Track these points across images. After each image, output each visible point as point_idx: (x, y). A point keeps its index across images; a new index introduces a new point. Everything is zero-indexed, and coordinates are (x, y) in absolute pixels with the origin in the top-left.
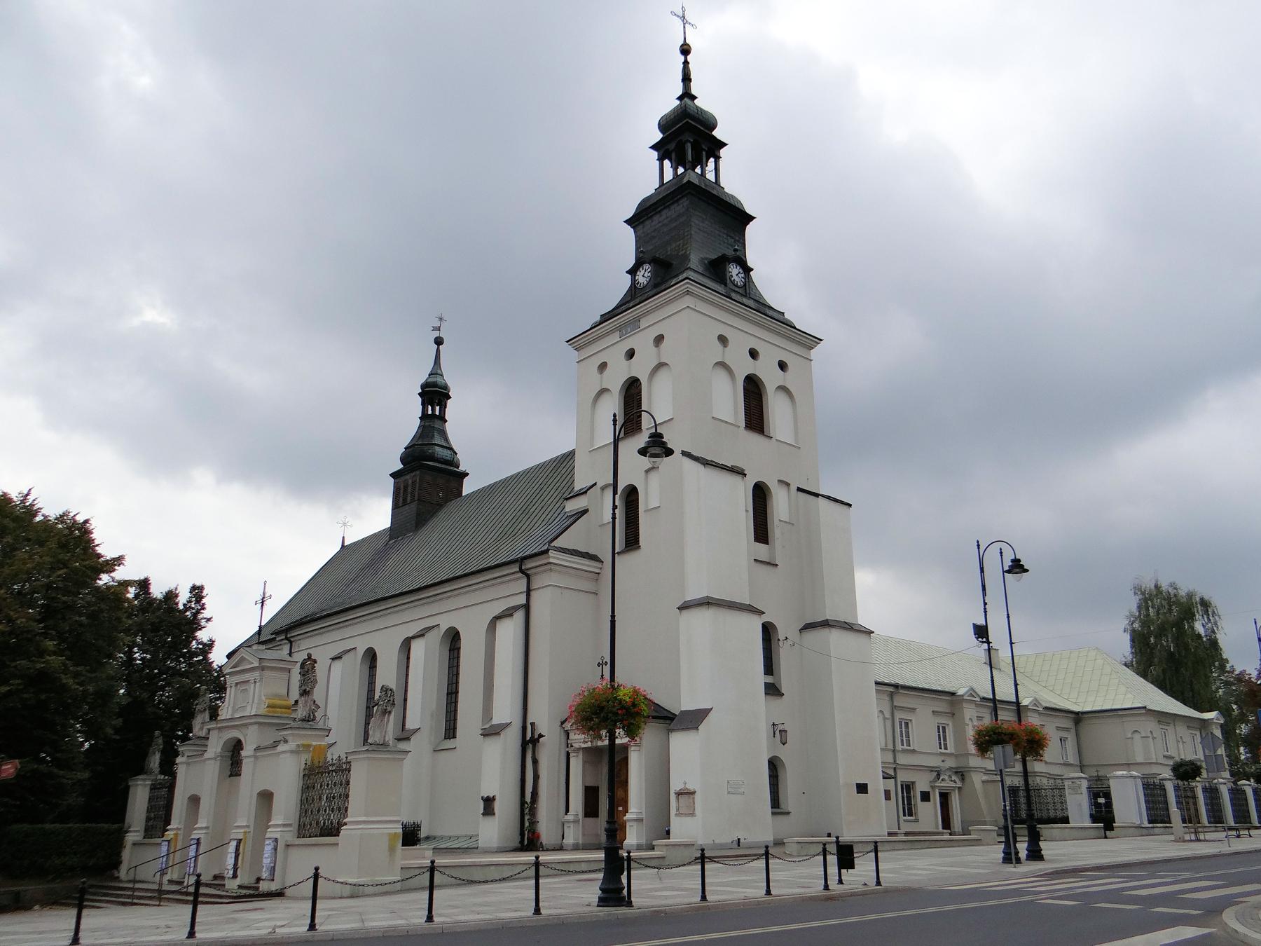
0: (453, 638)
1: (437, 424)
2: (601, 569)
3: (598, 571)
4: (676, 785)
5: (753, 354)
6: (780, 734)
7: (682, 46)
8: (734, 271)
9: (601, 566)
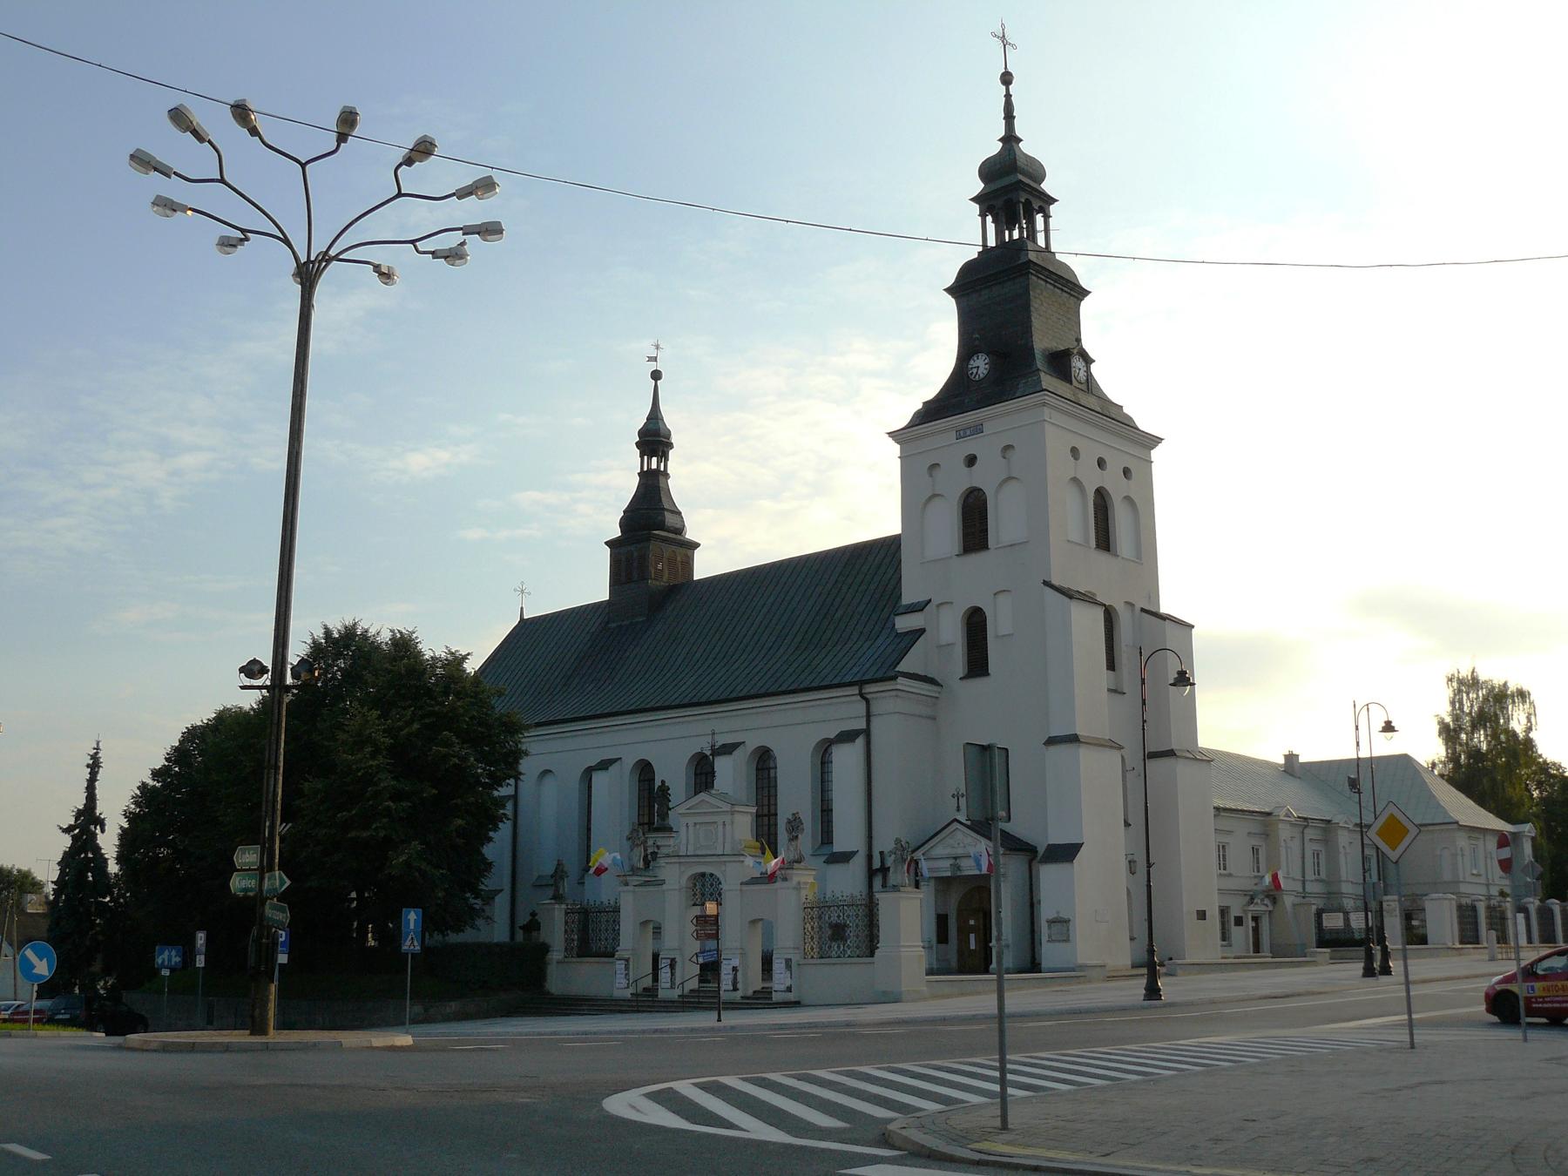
0: (764, 761)
2: (939, 693)
3: (937, 695)
4: (1046, 912)
5: (1101, 463)
7: (1003, 74)
8: (1077, 363)
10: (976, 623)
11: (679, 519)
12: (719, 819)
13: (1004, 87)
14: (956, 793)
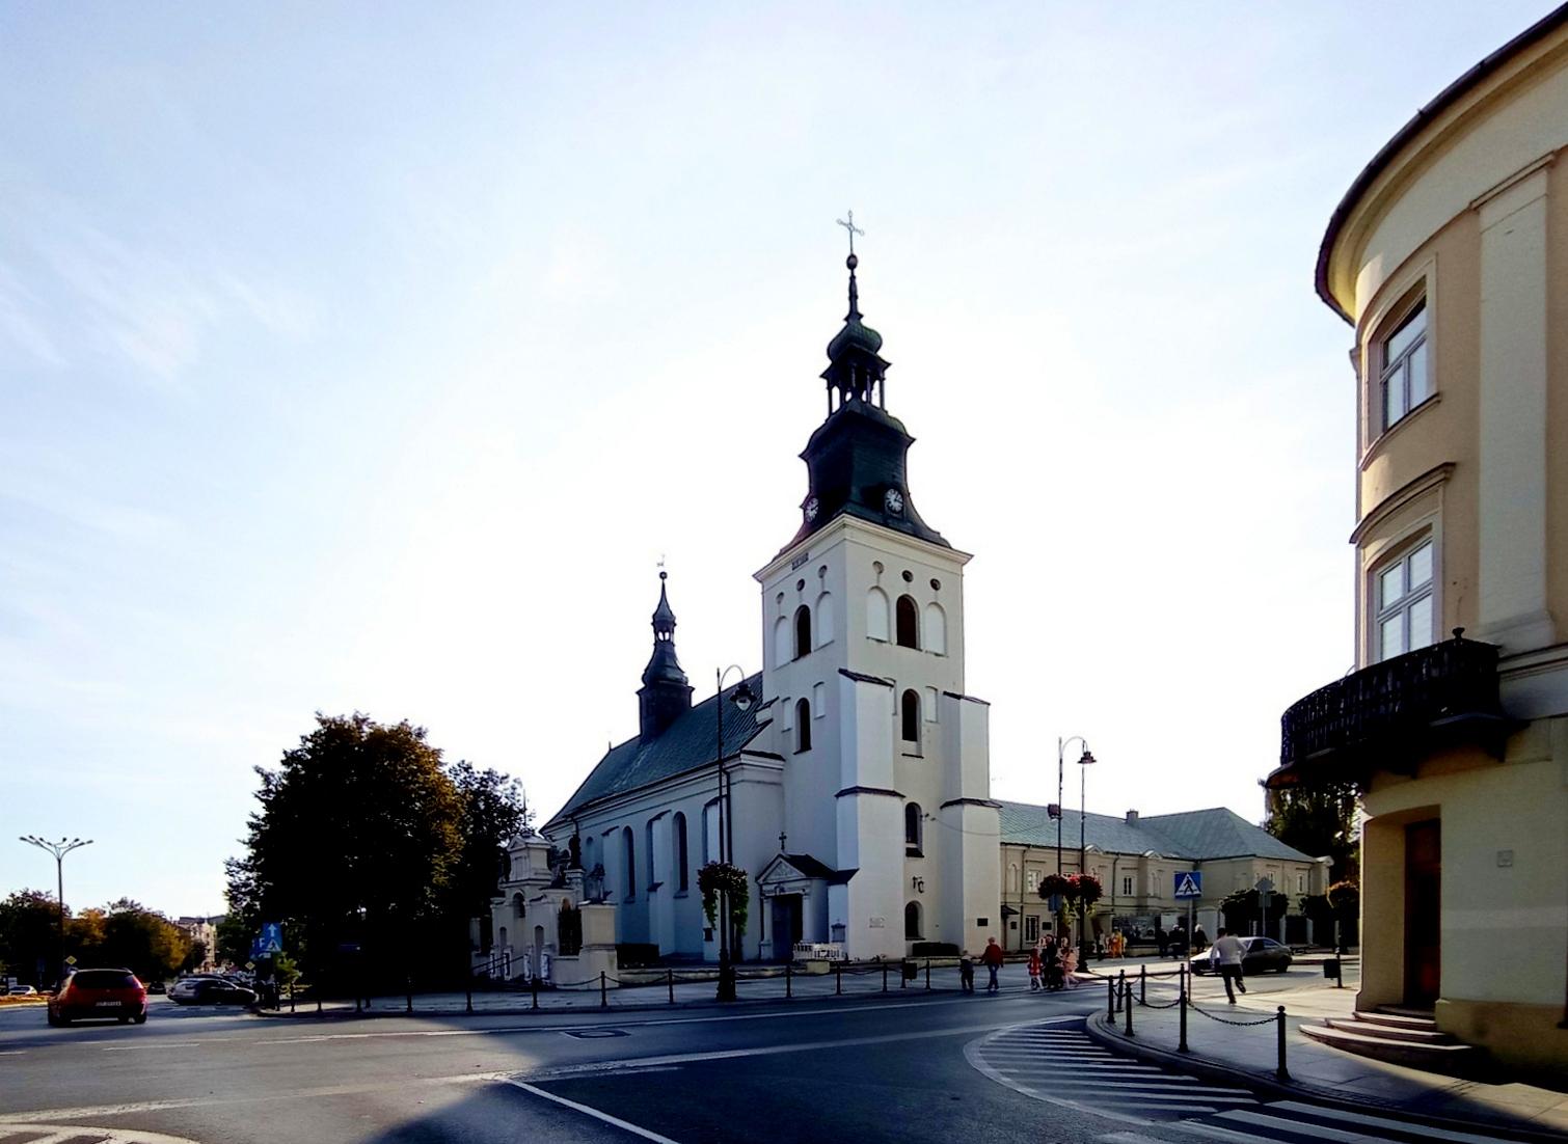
4: (832, 921)
5: (907, 576)
6: (917, 884)
8: (892, 497)
10: (804, 707)
13: (849, 271)
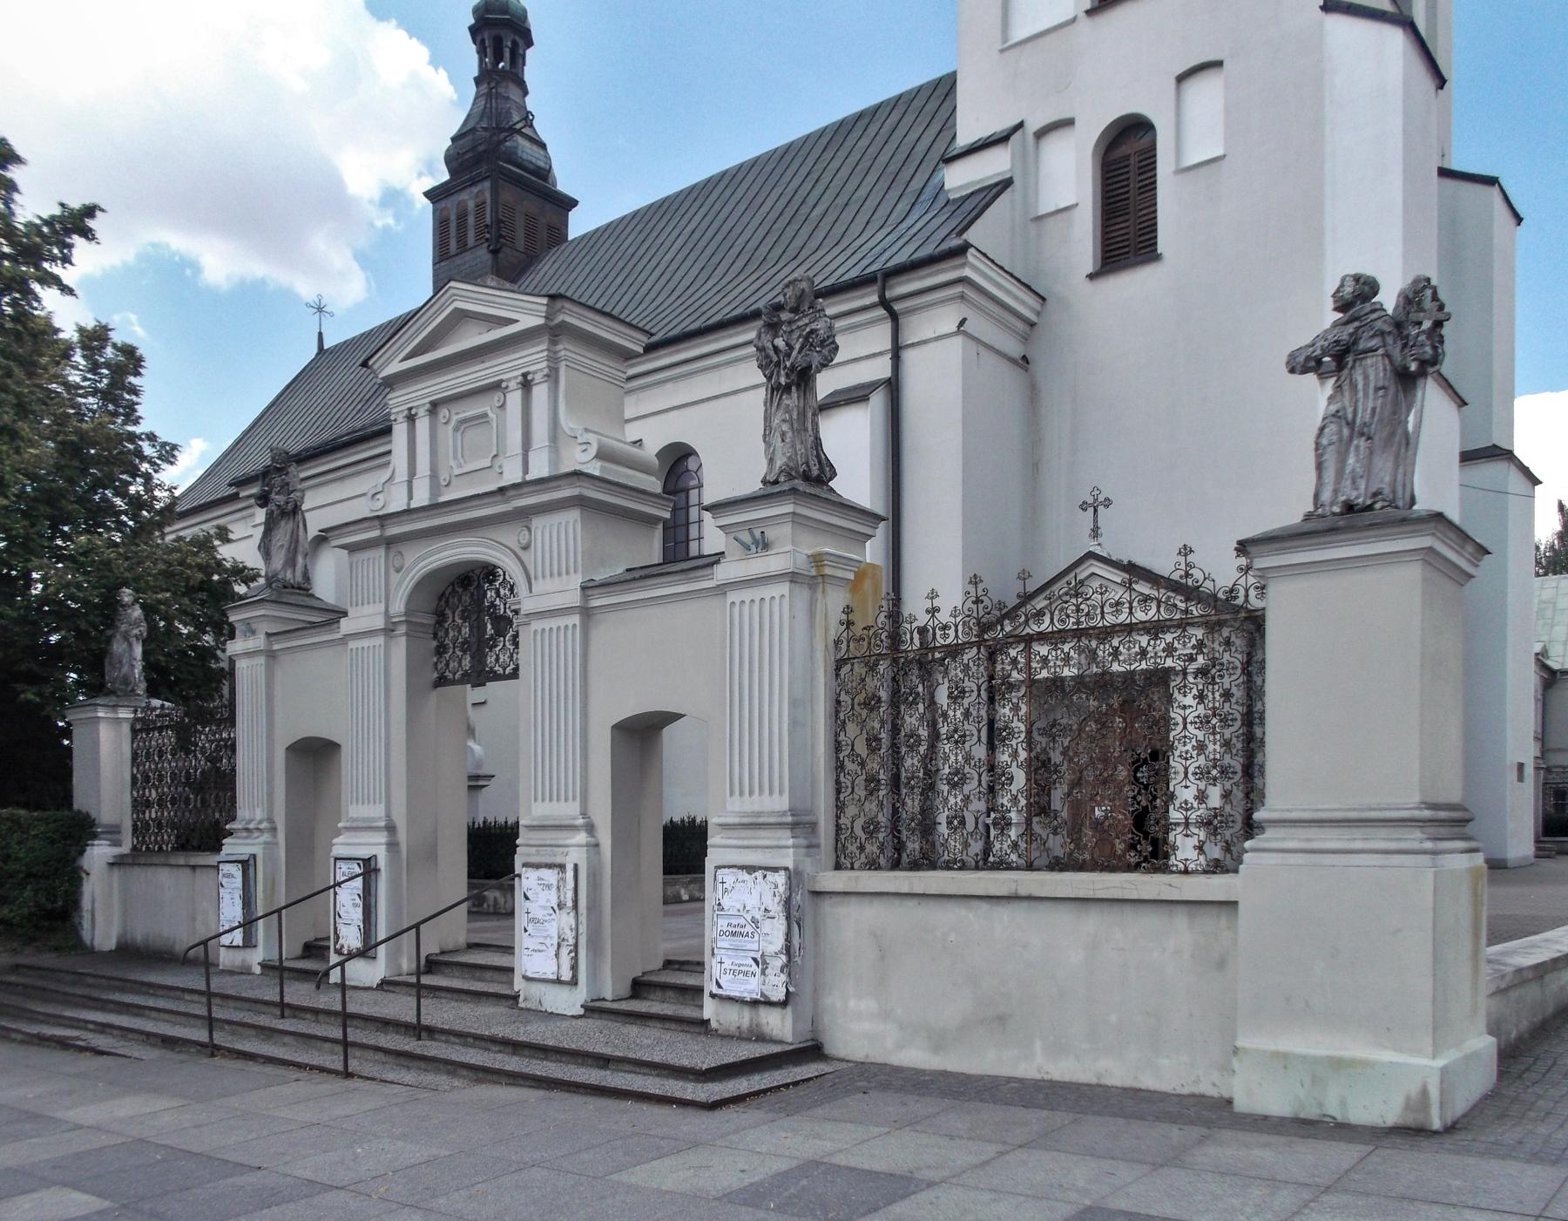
1: (513, 92)
2: (1038, 314)
3: (1033, 317)
9: (1037, 306)
11: (542, 152)
12: (507, 367)
14: (1090, 500)
